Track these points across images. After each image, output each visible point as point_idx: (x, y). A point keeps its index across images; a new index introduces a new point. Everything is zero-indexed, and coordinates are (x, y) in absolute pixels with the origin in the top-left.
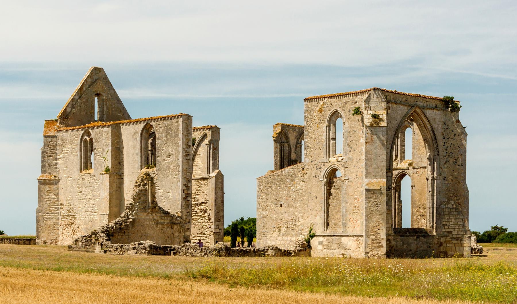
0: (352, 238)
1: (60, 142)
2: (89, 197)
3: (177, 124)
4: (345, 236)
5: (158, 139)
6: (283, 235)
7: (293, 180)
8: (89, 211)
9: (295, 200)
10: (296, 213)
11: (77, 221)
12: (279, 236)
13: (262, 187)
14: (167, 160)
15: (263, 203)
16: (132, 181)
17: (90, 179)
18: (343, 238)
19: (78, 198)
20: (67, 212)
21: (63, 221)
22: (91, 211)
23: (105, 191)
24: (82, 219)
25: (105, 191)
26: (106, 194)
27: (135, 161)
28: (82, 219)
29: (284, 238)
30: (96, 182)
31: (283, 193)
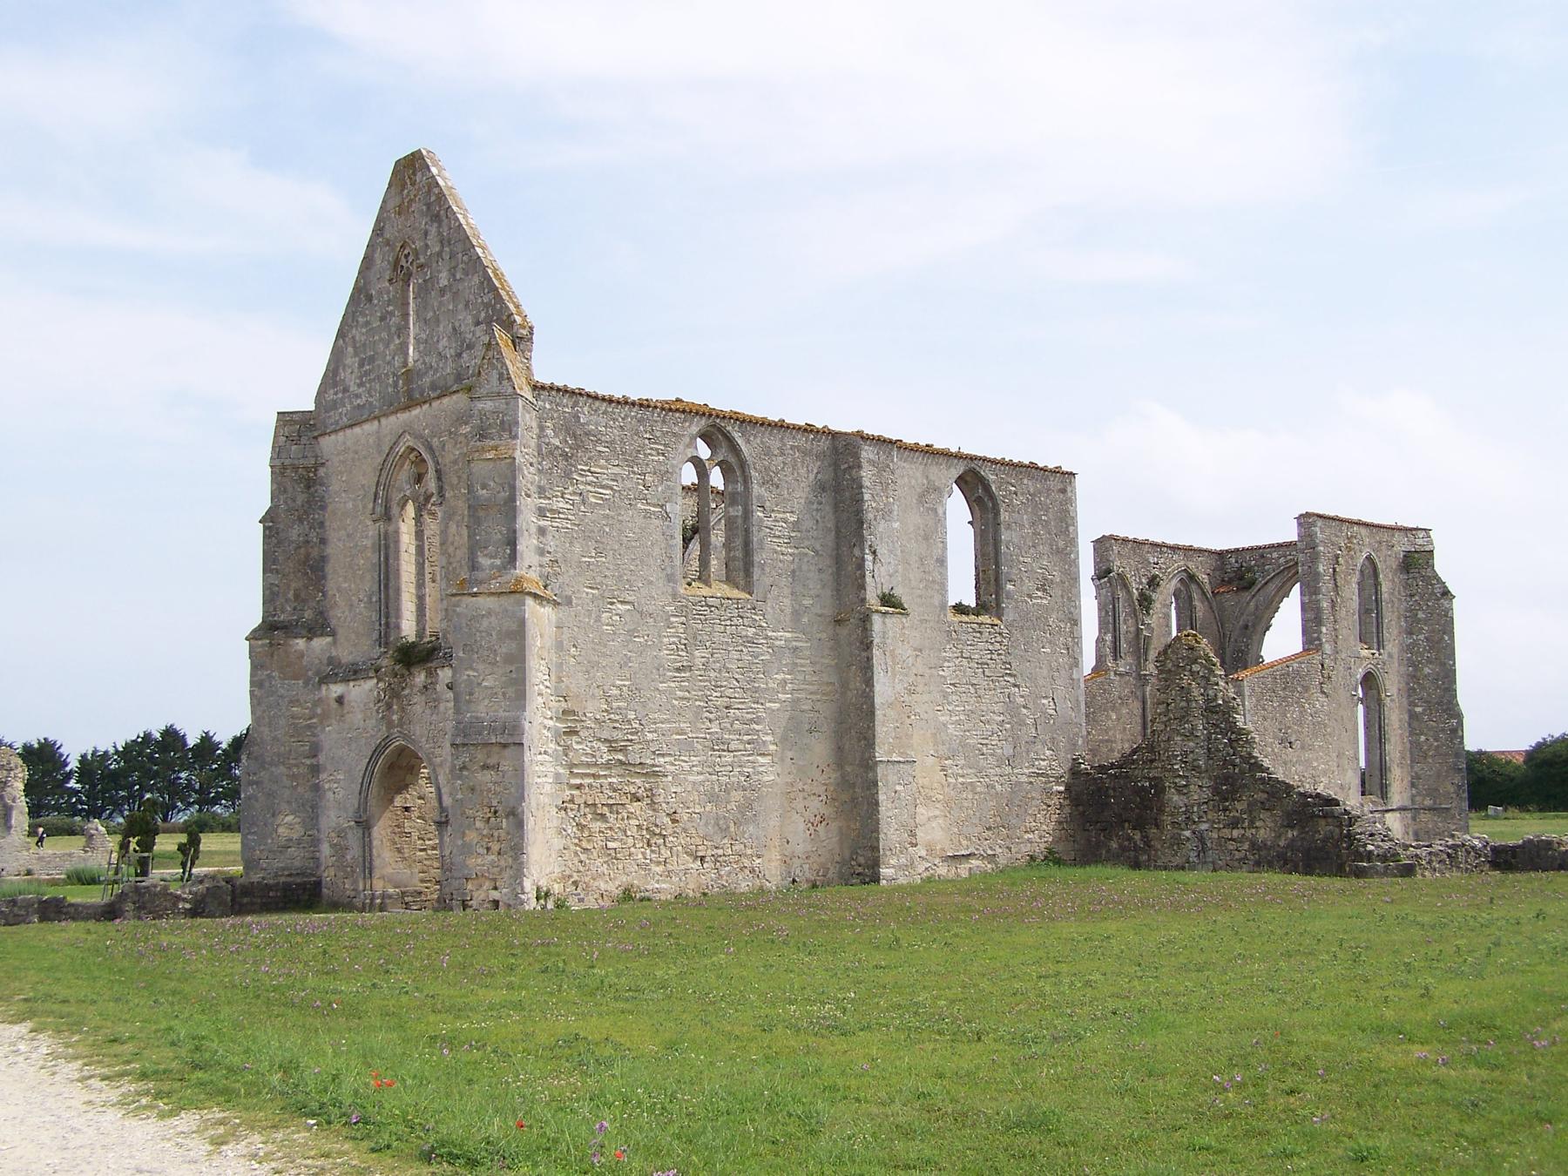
0: (1397, 814)
2: (729, 692)
3: (1062, 496)
5: (1009, 527)
7: (1306, 689)
8: (732, 747)
11: (668, 792)
14: (1036, 598)
17: (735, 621)
18: (1388, 815)
19: (671, 691)
21: (579, 787)
22: (741, 747)
23: (894, 675)
24: (691, 778)
25: (894, 675)
26: (899, 687)
27: (933, 581)
28: (691, 778)
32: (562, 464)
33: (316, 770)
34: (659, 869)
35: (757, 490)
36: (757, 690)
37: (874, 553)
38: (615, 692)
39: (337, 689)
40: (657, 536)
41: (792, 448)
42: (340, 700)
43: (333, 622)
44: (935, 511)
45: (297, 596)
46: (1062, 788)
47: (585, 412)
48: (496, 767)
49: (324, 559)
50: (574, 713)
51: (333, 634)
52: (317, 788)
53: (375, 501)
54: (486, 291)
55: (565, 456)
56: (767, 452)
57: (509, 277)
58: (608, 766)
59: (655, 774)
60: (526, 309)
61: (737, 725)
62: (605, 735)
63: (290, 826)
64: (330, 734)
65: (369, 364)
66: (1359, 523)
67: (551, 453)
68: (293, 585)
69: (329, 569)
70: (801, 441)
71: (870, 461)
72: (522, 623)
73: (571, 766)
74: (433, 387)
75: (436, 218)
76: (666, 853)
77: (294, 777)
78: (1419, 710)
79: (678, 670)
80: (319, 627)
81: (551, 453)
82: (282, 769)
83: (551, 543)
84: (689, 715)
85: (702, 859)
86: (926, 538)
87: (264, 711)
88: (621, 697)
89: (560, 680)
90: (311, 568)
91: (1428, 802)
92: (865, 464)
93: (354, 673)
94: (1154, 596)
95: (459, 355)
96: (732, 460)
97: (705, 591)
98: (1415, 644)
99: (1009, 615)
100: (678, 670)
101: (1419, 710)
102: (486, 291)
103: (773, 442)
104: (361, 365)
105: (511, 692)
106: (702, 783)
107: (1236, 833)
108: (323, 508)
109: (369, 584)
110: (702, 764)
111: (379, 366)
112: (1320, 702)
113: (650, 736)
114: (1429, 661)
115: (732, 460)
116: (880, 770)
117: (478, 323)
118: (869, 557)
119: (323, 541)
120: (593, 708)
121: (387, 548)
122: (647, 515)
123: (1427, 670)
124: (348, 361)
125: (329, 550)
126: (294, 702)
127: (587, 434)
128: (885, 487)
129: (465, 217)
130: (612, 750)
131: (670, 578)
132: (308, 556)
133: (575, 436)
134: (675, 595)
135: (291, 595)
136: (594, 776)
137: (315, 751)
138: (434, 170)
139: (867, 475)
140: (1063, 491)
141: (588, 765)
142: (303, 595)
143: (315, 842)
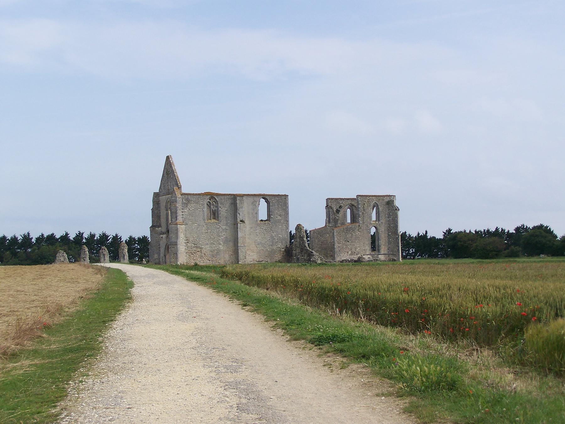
0: (383, 255)
1: (185, 202)
4: (380, 255)
6: (350, 255)
9: (356, 239)
10: (356, 245)
11: (204, 251)
12: (348, 255)
13: (337, 233)
15: (338, 241)
16: (252, 228)
18: (379, 255)
19: (204, 236)
20: (193, 245)
21: (189, 250)
23: (242, 232)
29: (350, 256)
30: (221, 227)
31: (349, 236)
32: (186, 205)
33: (160, 248)
34: (202, 262)
35: (219, 205)
36: (219, 235)
37: (239, 214)
38: (195, 237)
39: (162, 236)
40: (202, 214)
41: (226, 198)
42: (162, 237)
43: (162, 225)
44: (255, 205)
45: (157, 221)
46: (284, 250)
47: (189, 197)
48: (174, 248)
49: (160, 215)
50: (188, 240)
51: (161, 227)
52: (160, 250)
55: (186, 204)
56: (221, 199)
57: (179, 178)
58: (194, 247)
59: (202, 248)
60: (181, 183)
61: (216, 241)
62: (193, 243)
63: (156, 256)
64: (161, 242)
66: (372, 196)
67: (184, 204)
70: (228, 197)
71: (239, 200)
72: (177, 228)
73: (188, 247)
76: (203, 259)
78: (390, 234)
79: (205, 233)
80: (160, 226)
81: (184, 204)
82: (155, 248)
83: (184, 216)
84: (207, 239)
85: (210, 260)
86: (253, 210)
88: (196, 237)
89: (186, 235)
91: (391, 253)
92: (238, 200)
93: (163, 234)
94: (340, 210)
96: (215, 201)
97: (211, 221)
98: (390, 220)
99: (272, 221)
100: (205, 233)
101: (390, 234)
103: (223, 197)
105: (176, 238)
106: (210, 249)
107: (303, 257)
108: (160, 208)
109: (165, 220)
110: (210, 246)
112: (358, 233)
113: (200, 243)
114: (392, 223)
115: (215, 201)
116: (239, 247)
118: (238, 215)
119: (160, 213)
120: (191, 239)
121: (167, 215)
122: (200, 211)
123: (392, 225)
125: (161, 215)
126: (156, 237)
127: (190, 200)
128: (242, 203)
129: (174, 167)
130: (194, 245)
131: (204, 220)
133: (188, 201)
134: (205, 222)
136: (191, 248)
137: (159, 245)
138: (170, 159)
139: (238, 202)
140: (286, 199)
141: (190, 247)
143: (160, 259)
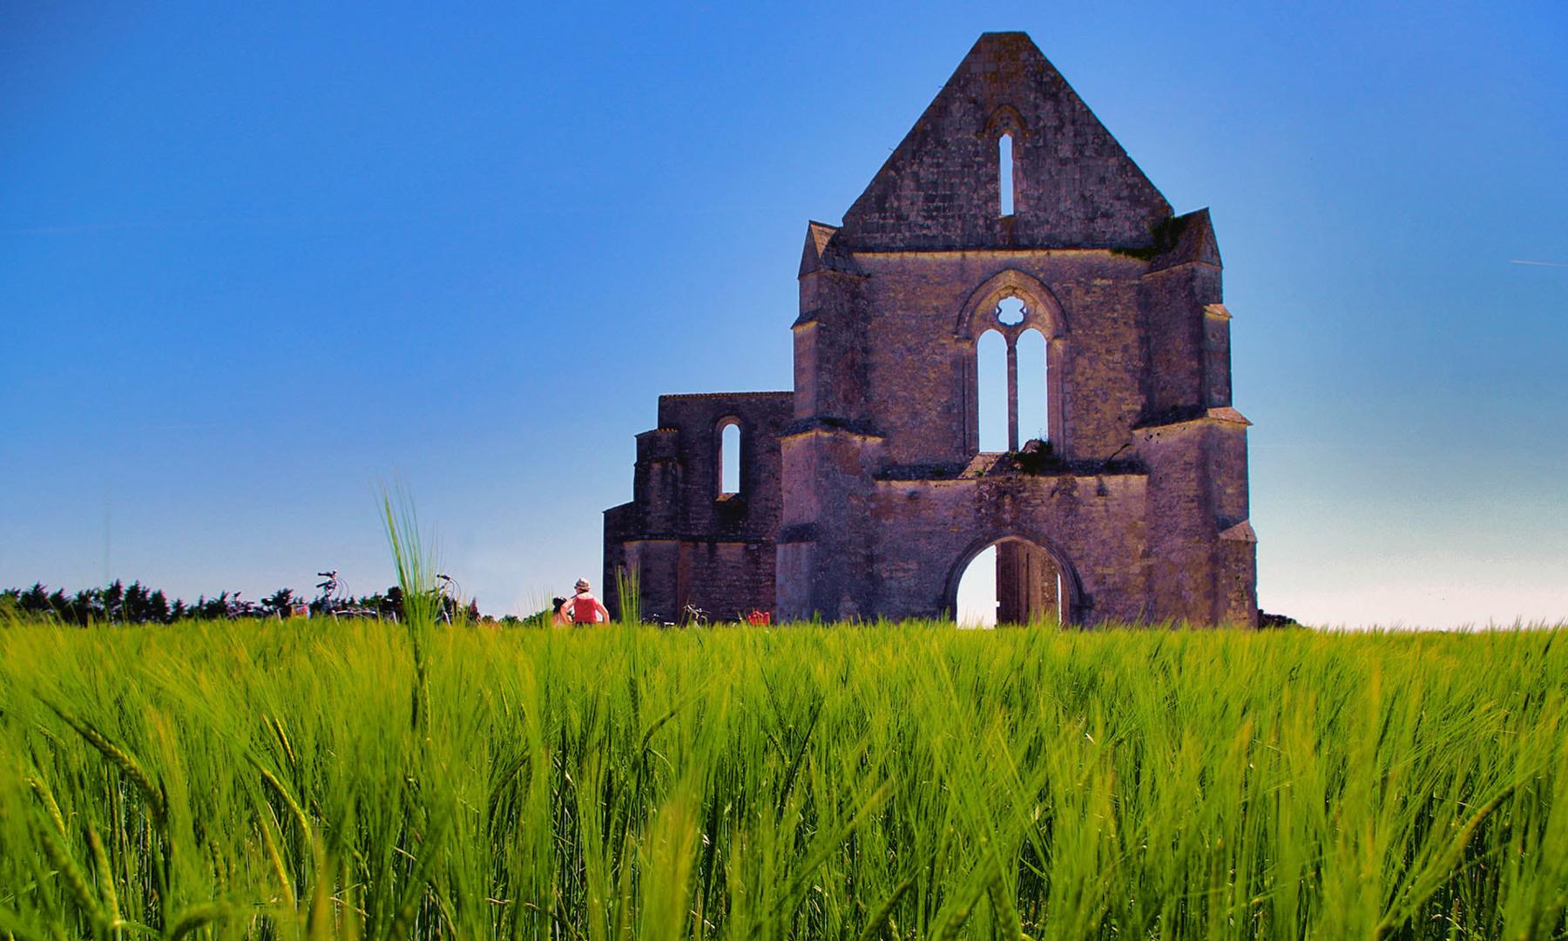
42: (913, 497)
45: (846, 397)
53: (958, 325)
54: (1130, 174)
65: (941, 201)
68: (843, 386)
69: (874, 377)
74: (1049, 237)
75: (1054, 97)
77: (855, 565)
82: (844, 558)
87: (829, 502)
90: (856, 372)
95: (1092, 220)
102: (1130, 174)
104: (929, 199)
111: (961, 207)
117: (1118, 198)
119: (866, 351)
121: (966, 368)
124: (906, 193)
132: (853, 360)
135: (840, 395)
142: (850, 396)
